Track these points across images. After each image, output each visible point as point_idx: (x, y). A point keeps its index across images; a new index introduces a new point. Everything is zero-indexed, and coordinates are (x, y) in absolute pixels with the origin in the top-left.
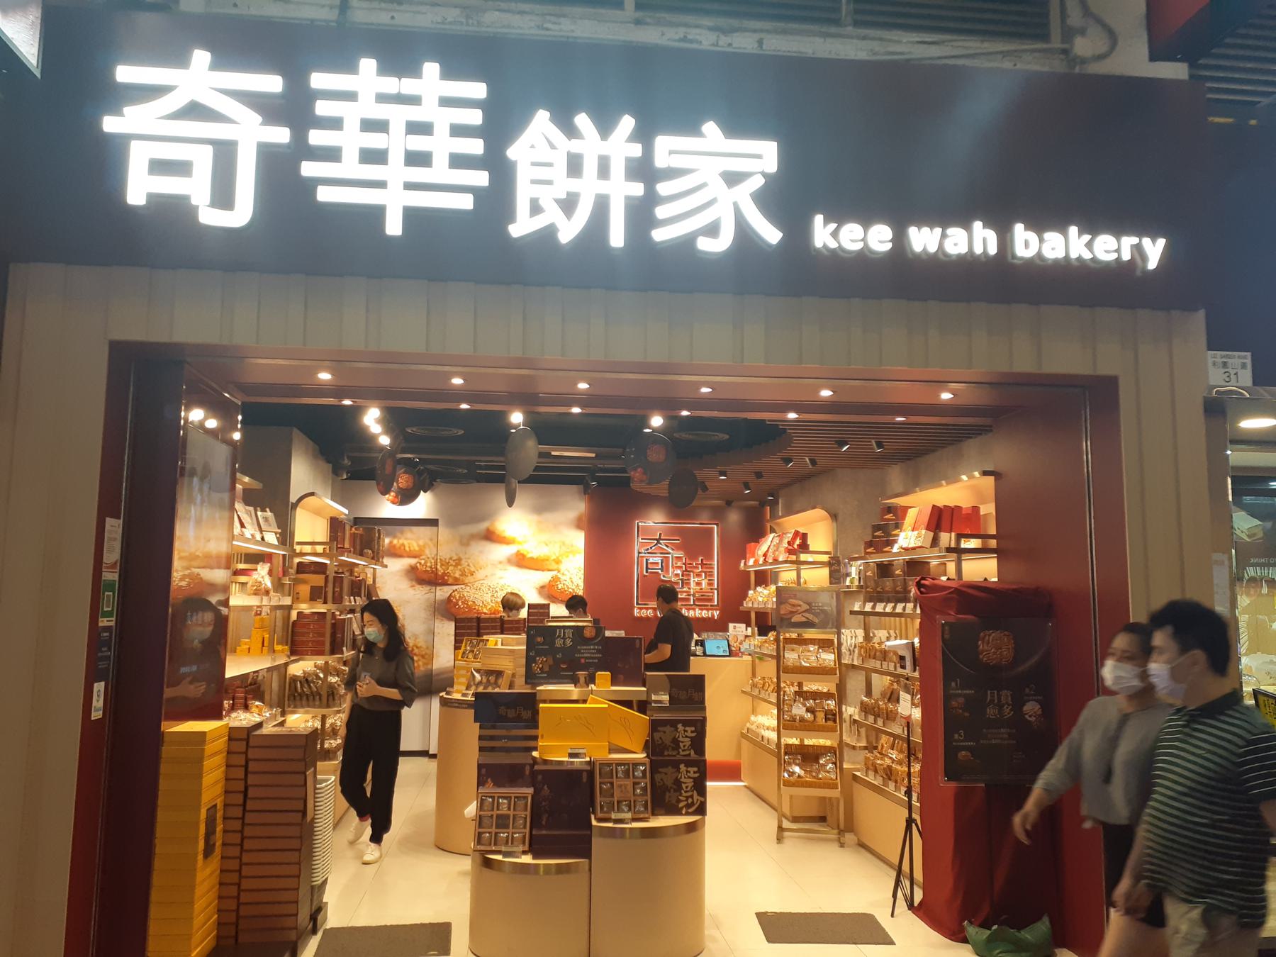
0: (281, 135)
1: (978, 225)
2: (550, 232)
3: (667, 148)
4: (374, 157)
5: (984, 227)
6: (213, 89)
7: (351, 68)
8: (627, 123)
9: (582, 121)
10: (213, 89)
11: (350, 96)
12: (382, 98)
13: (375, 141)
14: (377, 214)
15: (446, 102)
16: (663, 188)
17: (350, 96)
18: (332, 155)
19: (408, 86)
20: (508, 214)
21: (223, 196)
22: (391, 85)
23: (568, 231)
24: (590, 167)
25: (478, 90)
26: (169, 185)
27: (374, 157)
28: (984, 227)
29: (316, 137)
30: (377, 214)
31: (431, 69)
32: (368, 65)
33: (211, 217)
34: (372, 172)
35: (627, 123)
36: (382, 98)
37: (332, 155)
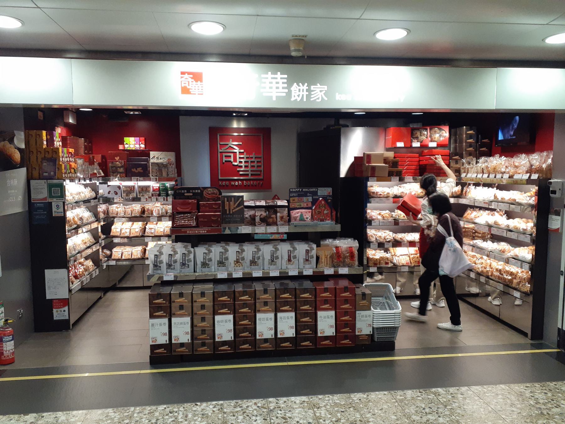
2: (296, 99)
4: (271, 88)
7: (267, 74)
11: (267, 78)
12: (272, 78)
14: (271, 97)
15: (281, 78)
17: (267, 78)
19: (275, 76)
20: (290, 97)
22: (273, 76)
23: (299, 99)
25: (286, 76)
27: (271, 88)
30: (271, 97)
36: (272, 78)
37: (265, 88)
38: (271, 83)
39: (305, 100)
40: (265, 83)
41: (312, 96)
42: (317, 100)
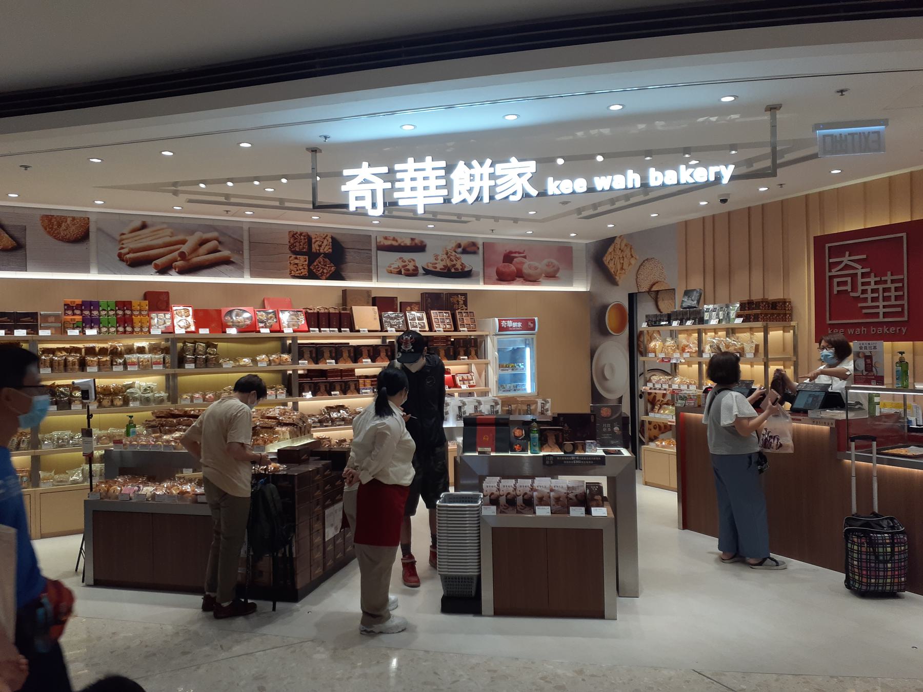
0: (389, 185)
1: (630, 172)
3: (500, 168)
4: (413, 189)
5: (634, 173)
6: (373, 174)
8: (488, 162)
9: (475, 163)
10: (373, 174)
13: (414, 184)
16: (499, 182)
18: (401, 190)
21: (374, 206)
23: (471, 199)
24: (477, 177)
26: (360, 204)
27: (413, 189)
28: (634, 173)
29: (398, 185)
31: (429, 159)
32: (411, 160)
33: (372, 212)
34: (413, 194)
35: (488, 162)
38: (413, 179)
39: (486, 199)
40: (401, 180)
41: (498, 189)
42: (512, 198)
